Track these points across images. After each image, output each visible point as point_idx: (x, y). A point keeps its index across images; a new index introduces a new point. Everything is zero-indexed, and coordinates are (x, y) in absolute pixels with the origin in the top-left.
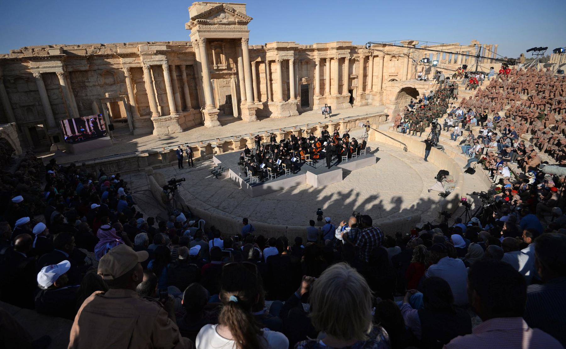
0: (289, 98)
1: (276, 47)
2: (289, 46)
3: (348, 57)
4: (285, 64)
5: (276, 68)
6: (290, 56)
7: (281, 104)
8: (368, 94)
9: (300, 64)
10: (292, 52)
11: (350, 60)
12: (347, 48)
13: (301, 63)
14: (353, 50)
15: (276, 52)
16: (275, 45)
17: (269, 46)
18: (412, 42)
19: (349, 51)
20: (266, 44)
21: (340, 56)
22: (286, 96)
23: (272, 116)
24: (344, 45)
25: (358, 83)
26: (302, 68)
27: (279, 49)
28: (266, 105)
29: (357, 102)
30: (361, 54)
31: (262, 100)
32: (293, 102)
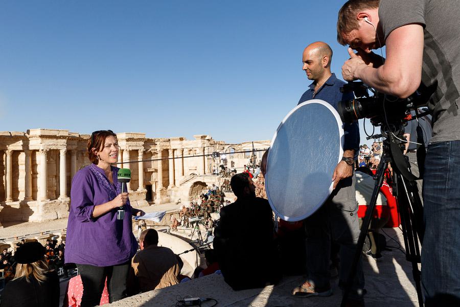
0: (58, 195)
1: (40, 134)
2: (61, 134)
3: (141, 150)
4: (52, 155)
5: (41, 159)
6: (61, 146)
7: (44, 203)
8: (170, 190)
9: (80, 155)
10: (65, 141)
11: (144, 153)
12: (140, 140)
13: (83, 154)
14: (149, 142)
15: (40, 140)
16: (38, 132)
17: (31, 133)
18: (205, 137)
19: (143, 143)
20: (28, 132)
21: (131, 149)
22: (53, 194)
23: (31, 219)
24: (136, 137)
25: (157, 178)
26: (83, 160)
27: (42, 137)
28: (24, 205)
29: (158, 199)
30: (158, 148)
31: (19, 198)
32: (63, 201)
